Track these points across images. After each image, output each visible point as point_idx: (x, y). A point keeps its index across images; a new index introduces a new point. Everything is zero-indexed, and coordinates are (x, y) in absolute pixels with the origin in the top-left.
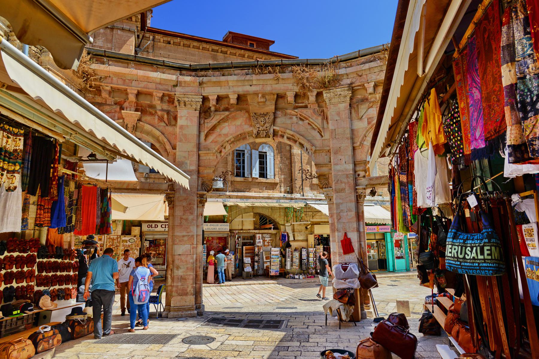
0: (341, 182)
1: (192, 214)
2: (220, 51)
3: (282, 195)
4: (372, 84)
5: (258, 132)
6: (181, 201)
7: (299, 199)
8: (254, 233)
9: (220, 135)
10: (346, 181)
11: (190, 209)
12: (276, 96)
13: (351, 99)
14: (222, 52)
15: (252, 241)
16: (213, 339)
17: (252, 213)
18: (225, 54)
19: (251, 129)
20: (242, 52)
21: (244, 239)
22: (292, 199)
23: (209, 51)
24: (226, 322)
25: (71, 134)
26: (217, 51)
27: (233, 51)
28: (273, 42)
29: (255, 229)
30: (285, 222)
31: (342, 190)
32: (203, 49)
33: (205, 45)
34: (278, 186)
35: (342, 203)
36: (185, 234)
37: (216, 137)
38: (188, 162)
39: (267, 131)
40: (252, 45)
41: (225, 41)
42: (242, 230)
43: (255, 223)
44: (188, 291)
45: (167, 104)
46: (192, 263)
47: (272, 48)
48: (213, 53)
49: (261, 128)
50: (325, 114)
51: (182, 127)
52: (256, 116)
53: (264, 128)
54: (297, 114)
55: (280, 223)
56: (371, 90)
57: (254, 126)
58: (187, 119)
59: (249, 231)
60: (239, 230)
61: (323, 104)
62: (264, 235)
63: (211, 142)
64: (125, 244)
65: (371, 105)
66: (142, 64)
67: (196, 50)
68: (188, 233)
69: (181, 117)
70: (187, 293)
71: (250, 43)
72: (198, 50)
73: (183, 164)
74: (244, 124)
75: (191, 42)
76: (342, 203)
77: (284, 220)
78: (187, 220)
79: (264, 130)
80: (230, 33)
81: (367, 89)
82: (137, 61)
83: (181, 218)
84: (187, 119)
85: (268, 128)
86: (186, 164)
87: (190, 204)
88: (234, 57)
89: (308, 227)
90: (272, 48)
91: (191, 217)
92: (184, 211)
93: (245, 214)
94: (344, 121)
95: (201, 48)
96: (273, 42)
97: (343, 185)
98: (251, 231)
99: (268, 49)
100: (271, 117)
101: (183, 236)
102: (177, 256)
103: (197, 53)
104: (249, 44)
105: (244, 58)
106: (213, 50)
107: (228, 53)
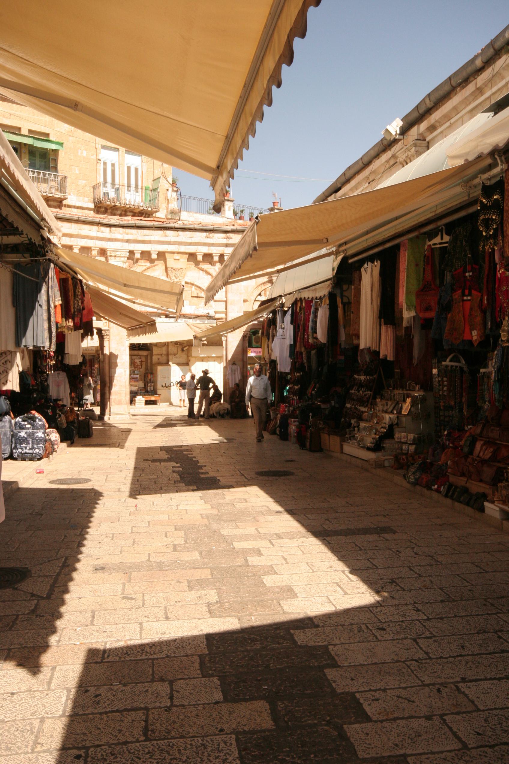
89: (185, 349)
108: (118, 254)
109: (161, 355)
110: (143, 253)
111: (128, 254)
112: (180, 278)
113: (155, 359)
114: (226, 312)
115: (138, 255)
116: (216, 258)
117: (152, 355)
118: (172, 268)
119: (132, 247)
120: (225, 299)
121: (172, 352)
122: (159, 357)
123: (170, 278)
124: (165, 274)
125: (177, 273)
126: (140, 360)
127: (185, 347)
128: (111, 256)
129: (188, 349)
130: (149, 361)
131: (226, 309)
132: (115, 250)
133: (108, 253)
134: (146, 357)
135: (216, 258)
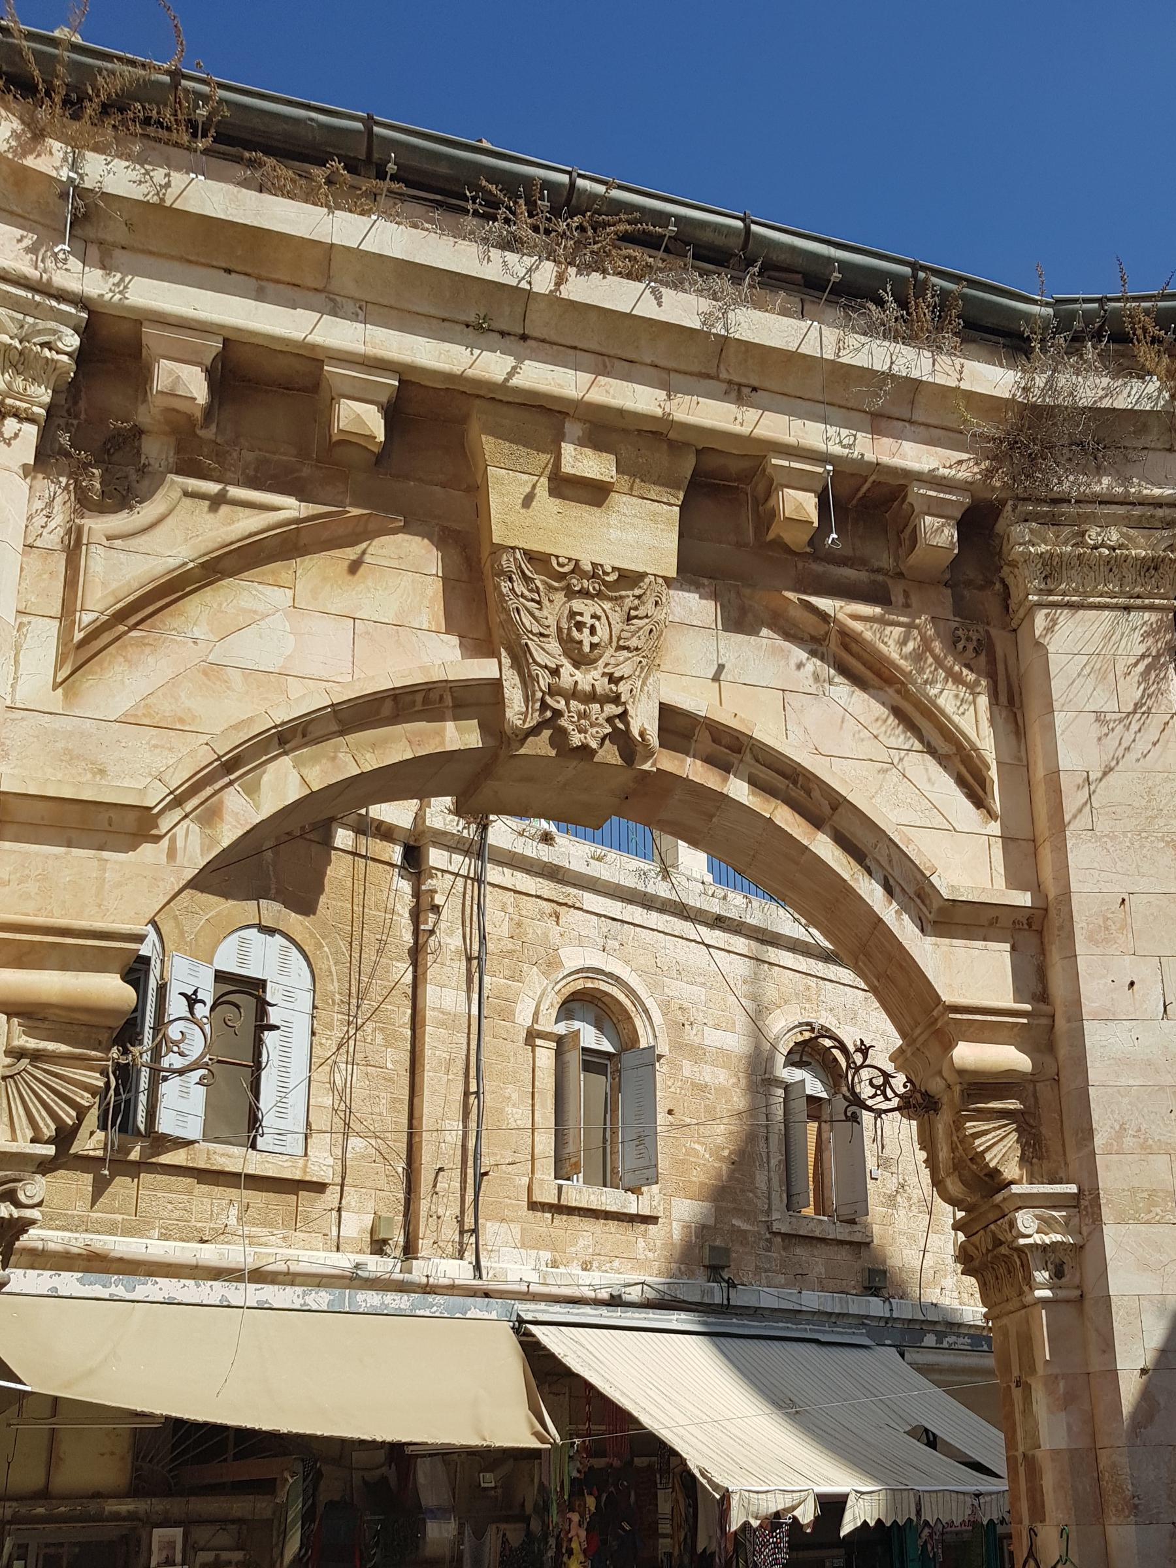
3: (343, 1261)
5: (544, 706)
7: (452, 1289)
8: (132, 1516)
19: (485, 669)
29: (136, 1490)
34: (332, 1195)
39: (612, 709)
42: (44, 1494)
49: (570, 676)
50: (1001, 667)
59: (93, 1507)
60: (19, 1498)
61: (990, 602)
79: (592, 697)
85: (623, 688)
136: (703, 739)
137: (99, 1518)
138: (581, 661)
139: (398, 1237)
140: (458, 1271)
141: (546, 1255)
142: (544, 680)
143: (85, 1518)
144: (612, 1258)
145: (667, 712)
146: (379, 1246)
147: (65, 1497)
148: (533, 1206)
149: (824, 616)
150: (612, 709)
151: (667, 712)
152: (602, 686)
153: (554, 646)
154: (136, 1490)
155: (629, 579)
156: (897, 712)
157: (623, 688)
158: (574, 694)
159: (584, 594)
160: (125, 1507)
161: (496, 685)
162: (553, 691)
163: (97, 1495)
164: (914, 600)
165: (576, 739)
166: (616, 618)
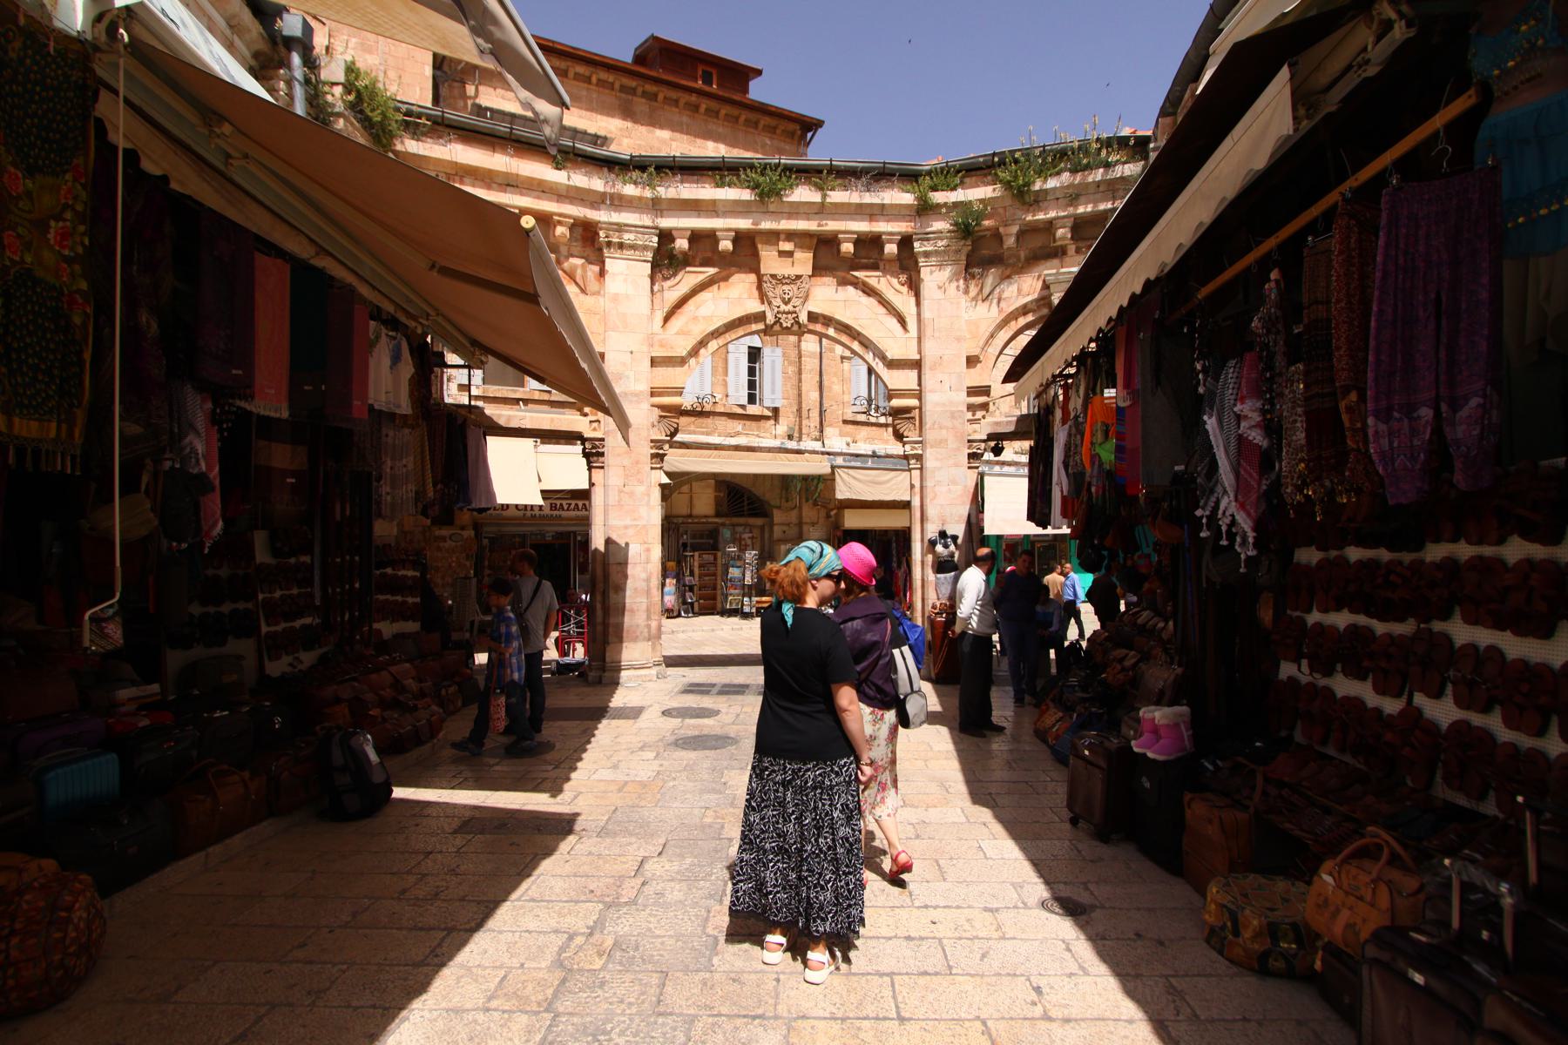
0: (941, 428)
1: (641, 482)
2: (640, 90)
3: (776, 443)
4: (1015, 229)
6: (619, 455)
9: (695, 318)
10: (949, 424)
11: (638, 472)
12: (815, 241)
13: (968, 256)
14: (645, 94)
15: (711, 541)
16: (717, 713)
17: (713, 481)
18: (651, 100)
20: (694, 98)
21: (694, 537)
22: (799, 452)
23: (613, 89)
24: (715, 690)
25: (428, 315)
26: (633, 91)
27: (673, 94)
28: (759, 73)
29: (718, 515)
30: (783, 500)
31: (941, 441)
32: (601, 83)
33: (603, 75)
35: (939, 469)
36: (628, 522)
37: (687, 323)
38: (631, 374)
39: (794, 315)
40: (708, 80)
41: (640, 58)
42: (690, 516)
43: (718, 503)
44: (638, 634)
45: (580, 243)
46: (644, 580)
47: (757, 91)
48: (623, 95)
49: (784, 308)
51: (616, 298)
52: (774, 282)
53: (789, 308)
54: (856, 281)
55: (773, 503)
56: (1010, 242)
57: (770, 303)
58: (625, 280)
60: (683, 517)
62: (740, 529)
63: (677, 333)
64: (441, 544)
65: (1008, 272)
66: (526, 146)
67: (582, 84)
68: (635, 519)
69: (614, 274)
70: (637, 637)
71: (703, 70)
72: (586, 85)
73: (620, 379)
74: (745, 296)
75: (569, 63)
76: (939, 469)
77: (781, 498)
78: (632, 494)
79: (789, 313)
80: (655, 39)
81: (1004, 238)
82: (514, 141)
83: (620, 492)
84: (625, 280)
85: (797, 309)
86: (628, 377)
87: (637, 462)
88: (674, 109)
90: (757, 91)
91: (641, 489)
92: (626, 476)
93: (699, 483)
94: (952, 303)
95: (594, 80)
96: (759, 73)
97: (944, 432)
98: (710, 520)
99: (746, 91)
100: (804, 285)
101: (626, 527)
102: (614, 567)
103: (584, 93)
104: (700, 73)
105: (696, 115)
106: (623, 89)
107: (661, 97)
108: (628, 237)
109: (788, 525)
110: (696, 237)
111: (656, 239)
112: (795, 302)
113: (778, 532)
114: (921, 391)
115: (682, 244)
116: (891, 249)
117: (772, 525)
118: (773, 276)
119: (666, 223)
120: (918, 357)
121: (808, 521)
122: (785, 528)
123: (770, 303)
124: (756, 293)
125: (786, 288)
126: (750, 535)
127: (832, 510)
128: (609, 244)
129: (836, 514)
130: (767, 535)
131: (920, 385)
132: (620, 228)
133: (602, 234)
134: (762, 528)
135: (891, 249)
136: (821, 320)
137: (707, 523)
138: (786, 303)
139: (796, 435)
140: (817, 446)
141: (849, 440)
142: (776, 309)
143: (703, 523)
144: (873, 439)
145: (810, 313)
146: (790, 437)
147: (697, 517)
148: (845, 422)
149: (857, 278)
150: (794, 315)
151: (810, 313)
152: (792, 309)
153: (779, 300)
154: (718, 515)
155: (798, 277)
156: (880, 302)
157: (797, 309)
158: (784, 313)
159: (786, 283)
160: (717, 520)
161: (764, 312)
162: (778, 312)
163: (706, 517)
164: (887, 267)
165: (785, 325)
166: (795, 288)
